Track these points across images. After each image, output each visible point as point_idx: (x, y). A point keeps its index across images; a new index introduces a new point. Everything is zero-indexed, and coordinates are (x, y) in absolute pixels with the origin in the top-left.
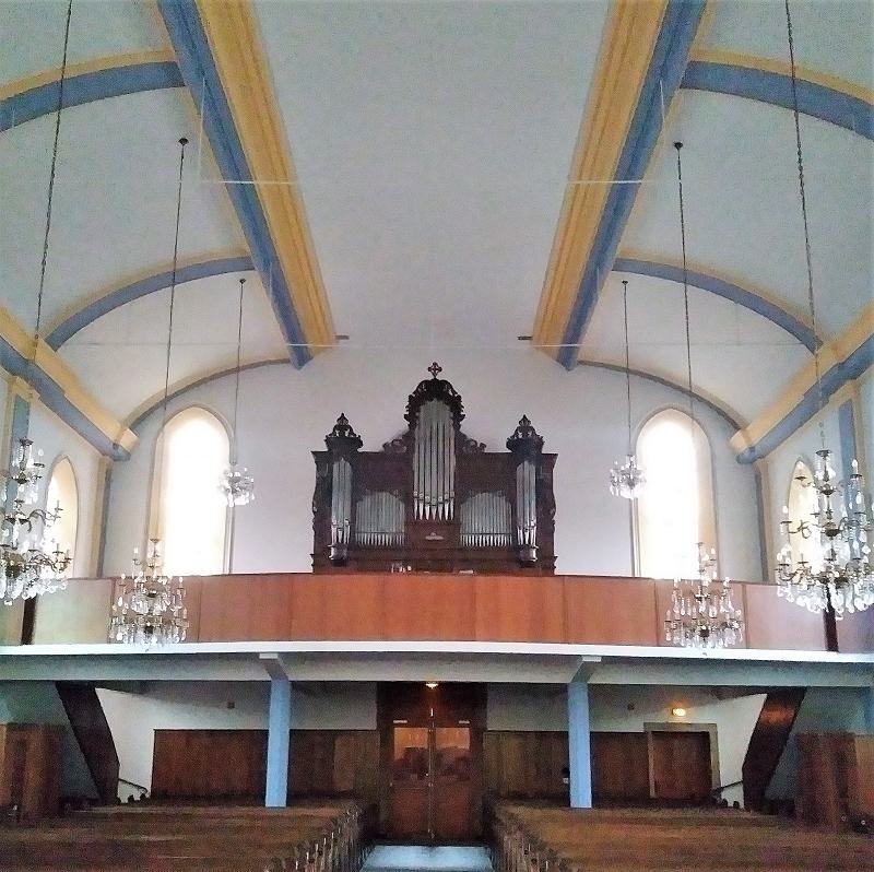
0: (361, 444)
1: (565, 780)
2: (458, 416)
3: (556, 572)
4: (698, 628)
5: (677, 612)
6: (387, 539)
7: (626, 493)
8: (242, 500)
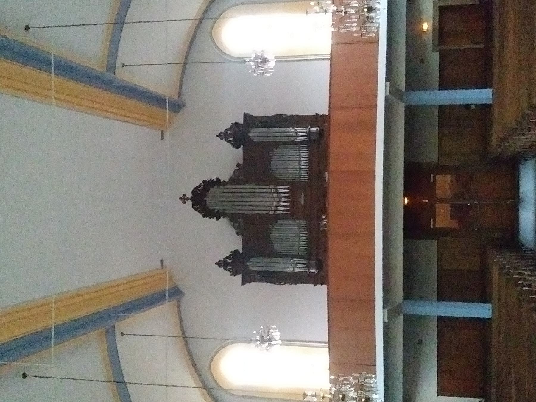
0: (237, 251)
1: (473, 107)
2: (217, 183)
3: (327, 113)
4: (367, 14)
5: (354, 29)
6: (303, 233)
7: (271, 64)
8: (276, 334)
